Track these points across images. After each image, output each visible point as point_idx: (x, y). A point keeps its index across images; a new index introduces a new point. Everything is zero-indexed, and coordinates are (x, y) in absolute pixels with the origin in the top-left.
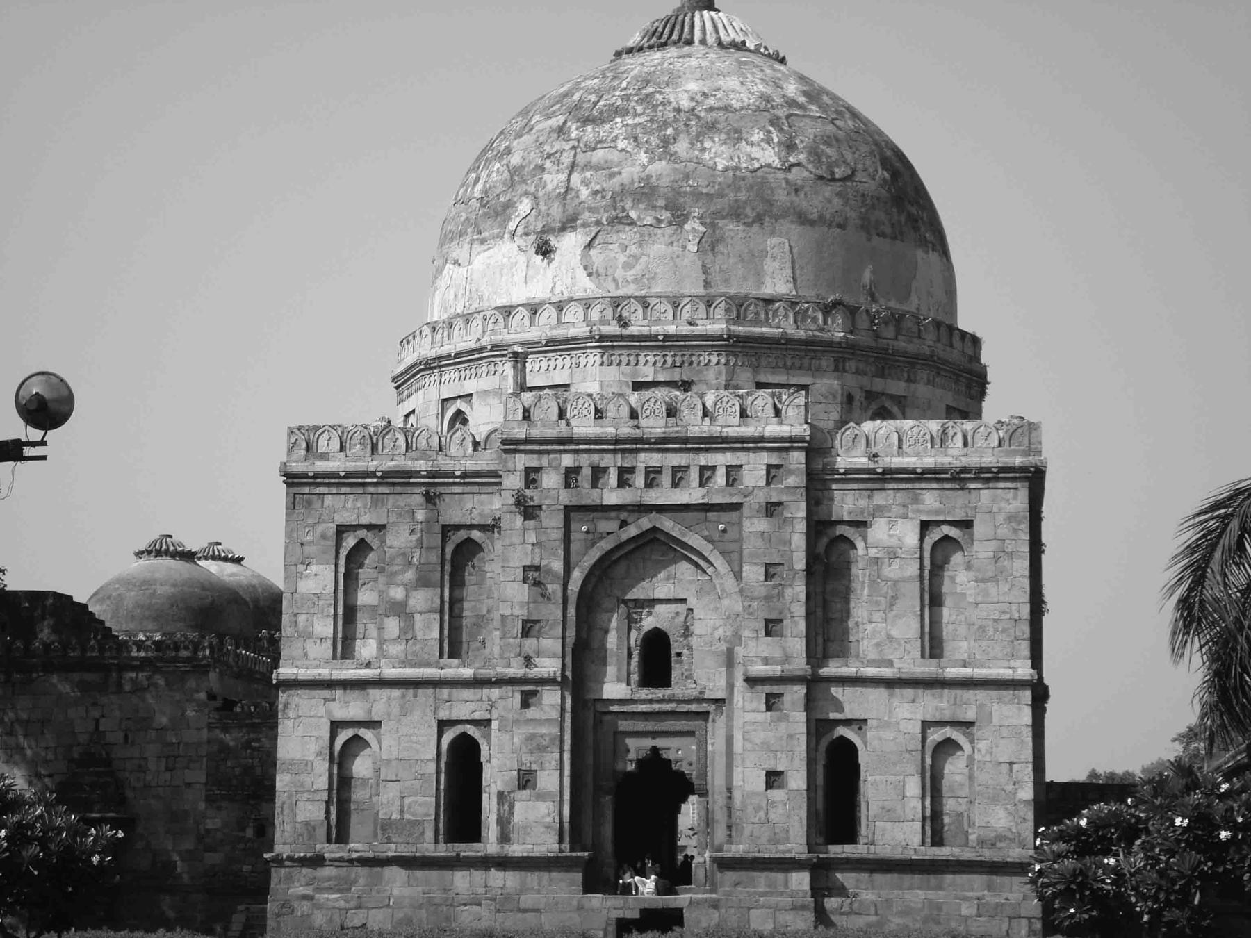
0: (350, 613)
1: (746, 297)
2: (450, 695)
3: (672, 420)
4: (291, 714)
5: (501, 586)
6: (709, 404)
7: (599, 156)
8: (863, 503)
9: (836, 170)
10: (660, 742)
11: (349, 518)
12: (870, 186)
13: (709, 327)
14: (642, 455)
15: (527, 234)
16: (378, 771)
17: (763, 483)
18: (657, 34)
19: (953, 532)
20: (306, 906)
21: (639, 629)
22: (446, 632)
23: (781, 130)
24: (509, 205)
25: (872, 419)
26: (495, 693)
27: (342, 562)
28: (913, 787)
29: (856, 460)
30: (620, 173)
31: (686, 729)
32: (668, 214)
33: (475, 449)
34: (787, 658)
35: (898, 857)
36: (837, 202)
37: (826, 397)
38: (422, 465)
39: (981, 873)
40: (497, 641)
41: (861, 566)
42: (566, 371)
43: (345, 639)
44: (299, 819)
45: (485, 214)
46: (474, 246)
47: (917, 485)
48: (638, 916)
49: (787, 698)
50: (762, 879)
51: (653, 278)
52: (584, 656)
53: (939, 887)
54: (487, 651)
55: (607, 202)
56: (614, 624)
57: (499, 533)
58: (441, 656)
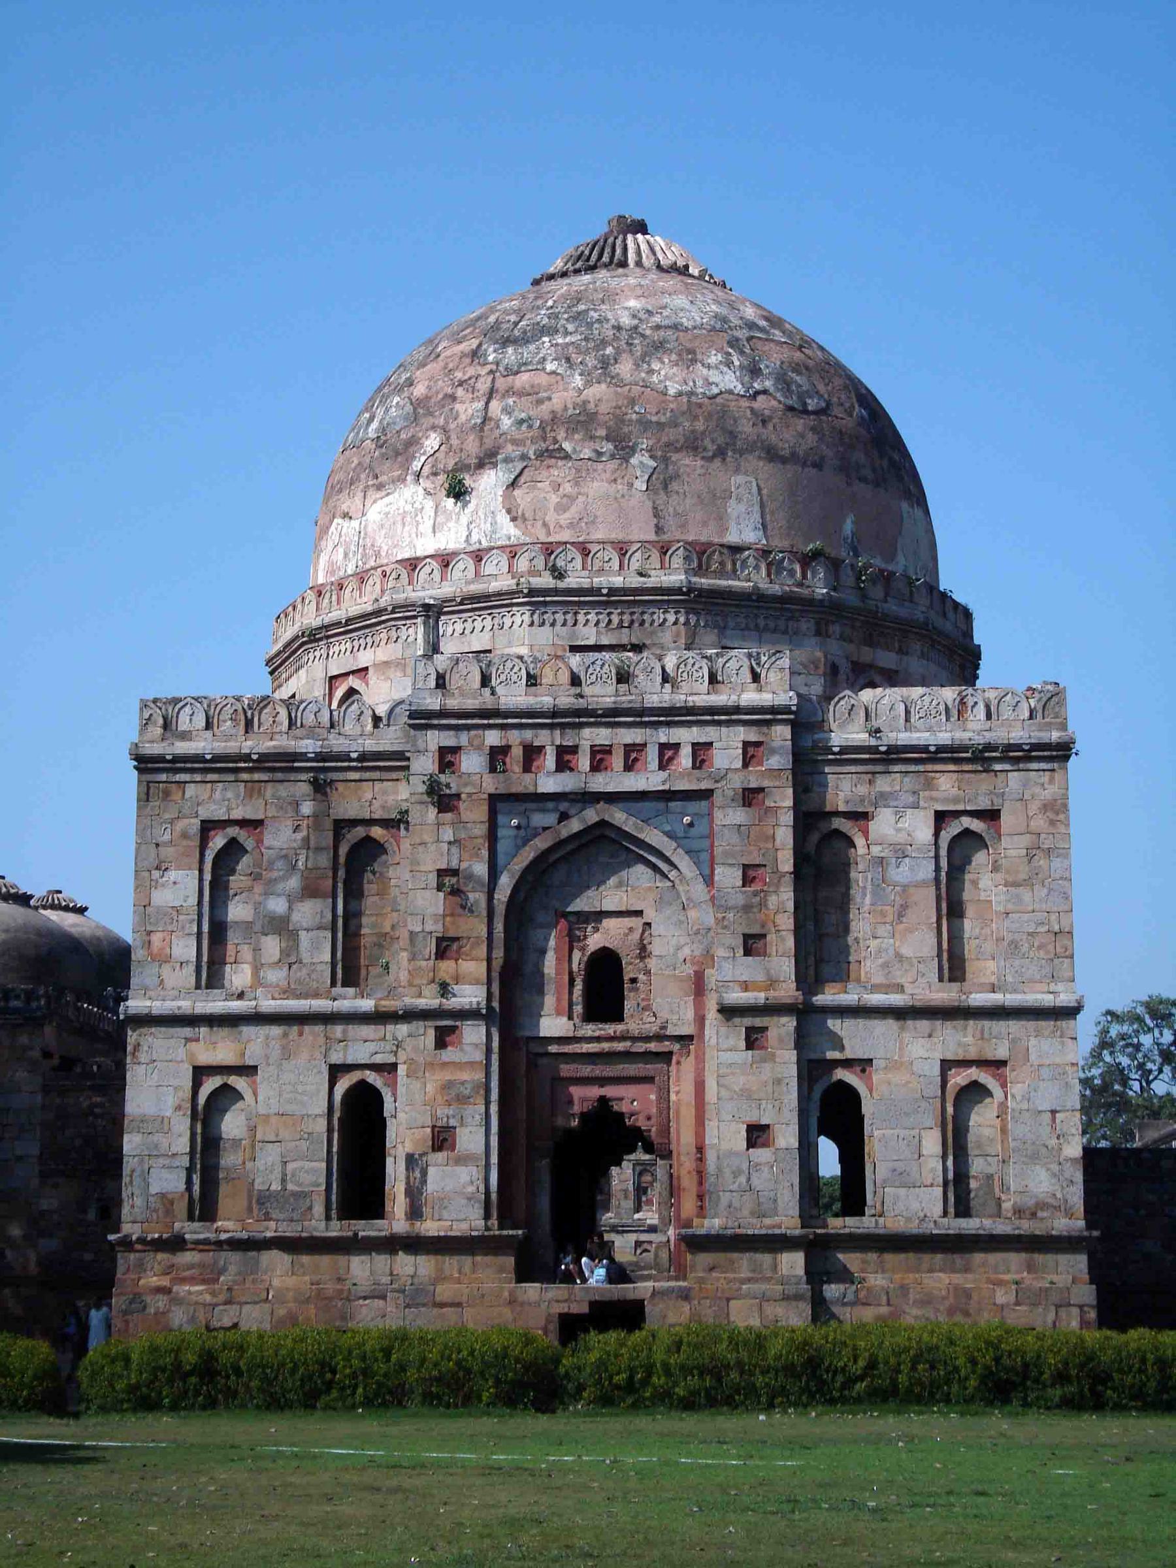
0: (216, 936)
1: (710, 544)
2: (344, 1032)
3: (623, 687)
4: (143, 1057)
5: (410, 895)
6: (670, 668)
7: (523, 380)
8: (862, 790)
9: (809, 401)
10: (609, 1091)
11: (220, 814)
12: (848, 423)
13: (663, 578)
14: (586, 732)
15: (435, 474)
16: (253, 1129)
17: (738, 764)
18: (584, 258)
19: (976, 825)
20: (161, 1302)
21: (583, 949)
23: (742, 353)
24: (413, 443)
25: (873, 685)
26: (403, 1029)
27: (208, 866)
28: (932, 1143)
29: (854, 736)
30: (550, 399)
31: (643, 1074)
32: (610, 446)
33: (376, 726)
34: (772, 983)
35: (915, 1231)
36: (811, 439)
37: (805, 667)
38: (308, 746)
39: (1018, 1250)
40: (405, 963)
41: (861, 867)
42: (487, 635)
43: (211, 963)
44: (154, 1189)
45: (382, 455)
46: (369, 493)
47: (929, 767)
48: (585, 1309)
49: (772, 1034)
50: (744, 1262)
51: (593, 522)
52: (514, 985)
53: (967, 1269)
54: (391, 977)
55: (535, 432)
56: (552, 943)
57: (407, 829)
58: (333, 983)
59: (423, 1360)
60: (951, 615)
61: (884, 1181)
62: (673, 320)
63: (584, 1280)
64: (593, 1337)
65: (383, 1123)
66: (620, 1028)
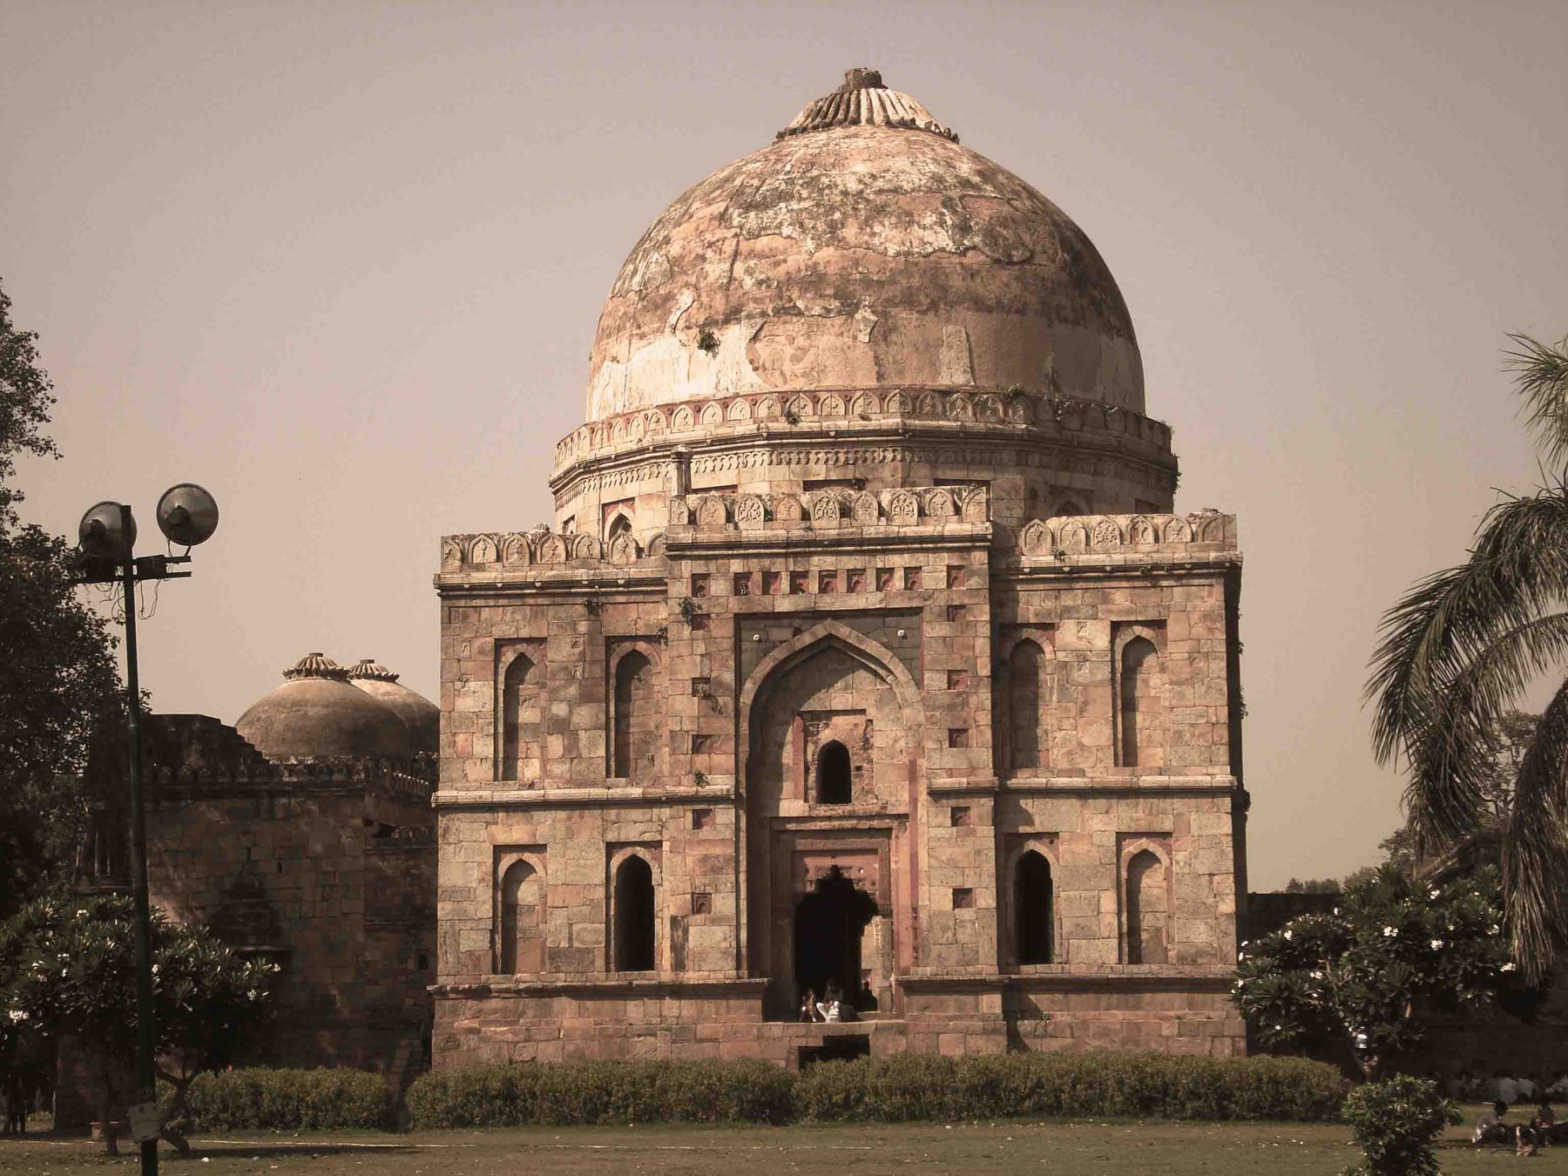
0: (510, 733)
1: (922, 388)
3: (846, 521)
5: (670, 700)
6: (885, 504)
7: (763, 243)
8: (1049, 604)
10: (841, 861)
11: (510, 633)
14: (815, 559)
15: (689, 328)
19: (1146, 633)
20: (473, 1040)
21: (816, 743)
22: (612, 749)
23: (955, 212)
24: (669, 297)
25: (1059, 514)
26: (666, 812)
27: (501, 678)
28: (1109, 902)
31: (867, 846)
33: (639, 556)
34: (973, 770)
38: (582, 574)
39: (1181, 991)
40: (667, 758)
42: (733, 472)
43: (506, 758)
44: (463, 948)
47: (1107, 584)
48: (821, 1044)
49: (973, 813)
50: (951, 1003)
52: (759, 775)
53: (1137, 1007)
55: (773, 292)
56: (789, 738)
58: (608, 775)
59: (681, 1085)
60: (1146, 432)
61: (1070, 934)
62: (895, 183)
63: (820, 1018)
64: (819, 1066)
65: (652, 889)
66: (848, 808)
